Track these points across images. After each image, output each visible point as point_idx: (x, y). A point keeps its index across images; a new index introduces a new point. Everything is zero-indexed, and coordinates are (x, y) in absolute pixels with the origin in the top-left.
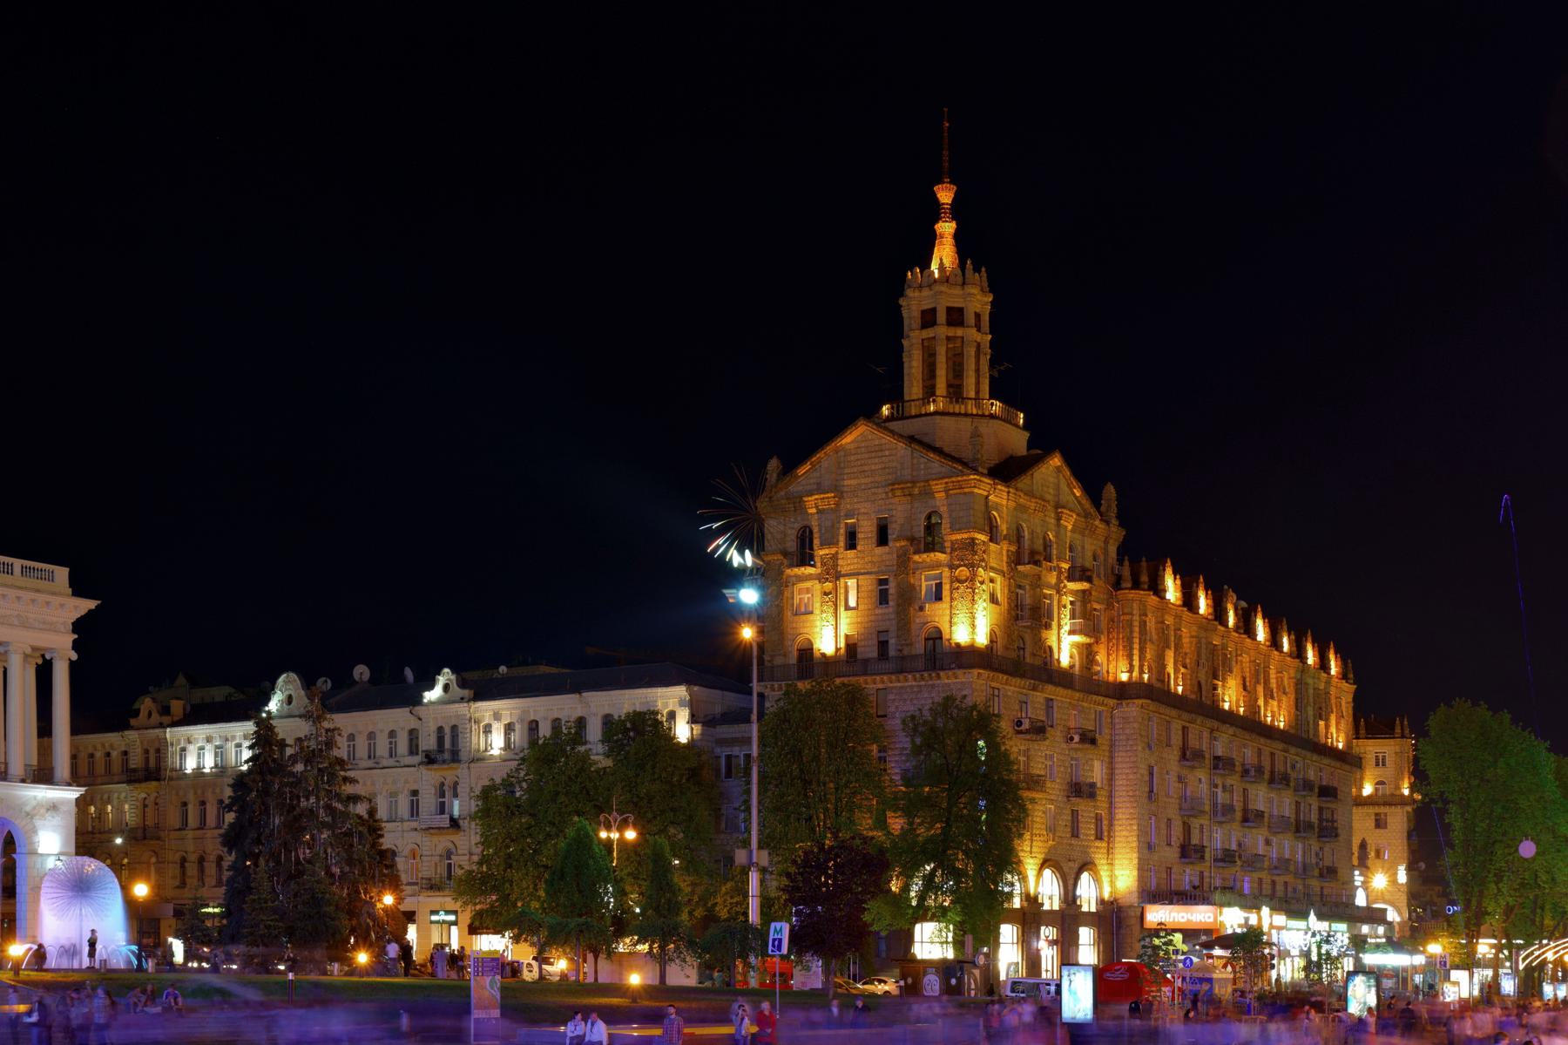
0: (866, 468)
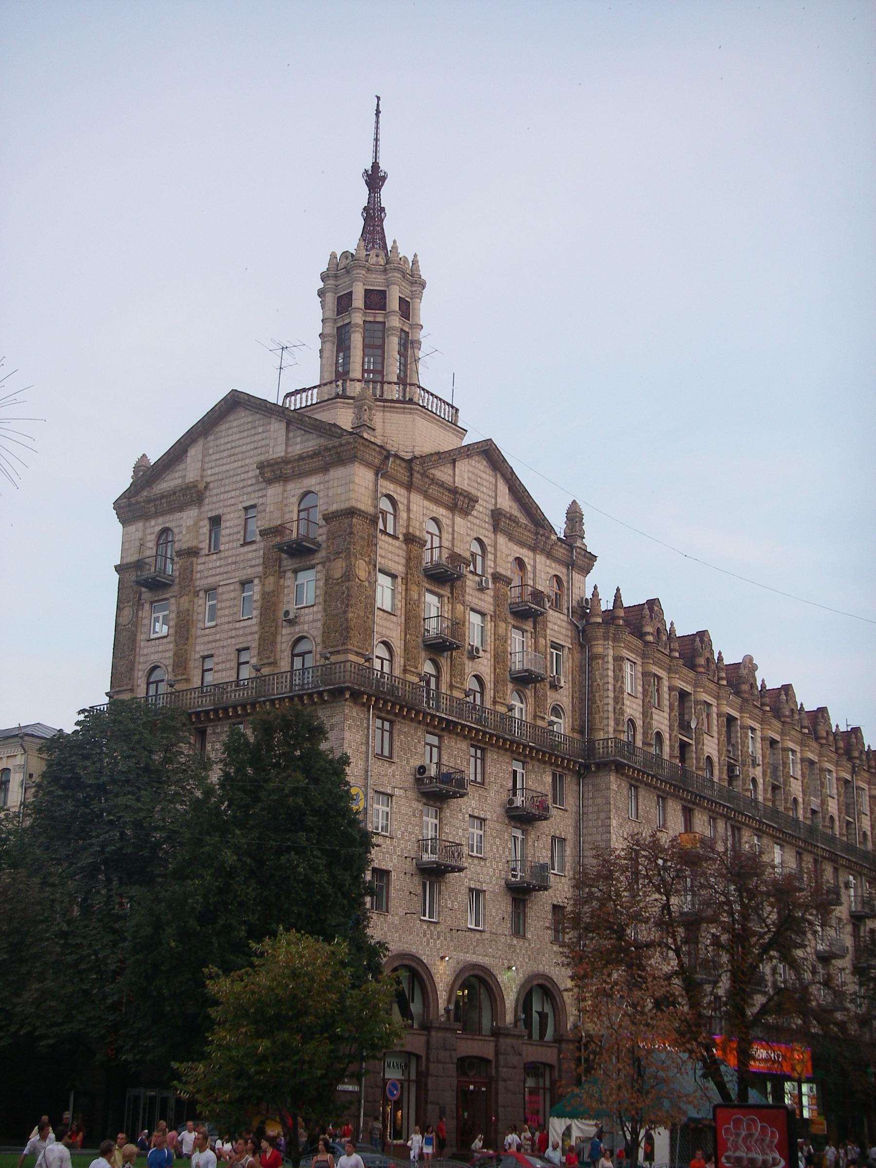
0: (237, 450)
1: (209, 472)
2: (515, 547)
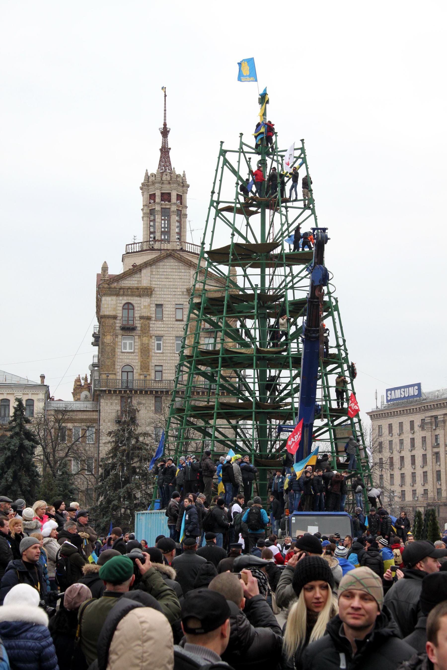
0: (170, 277)
1: (154, 283)
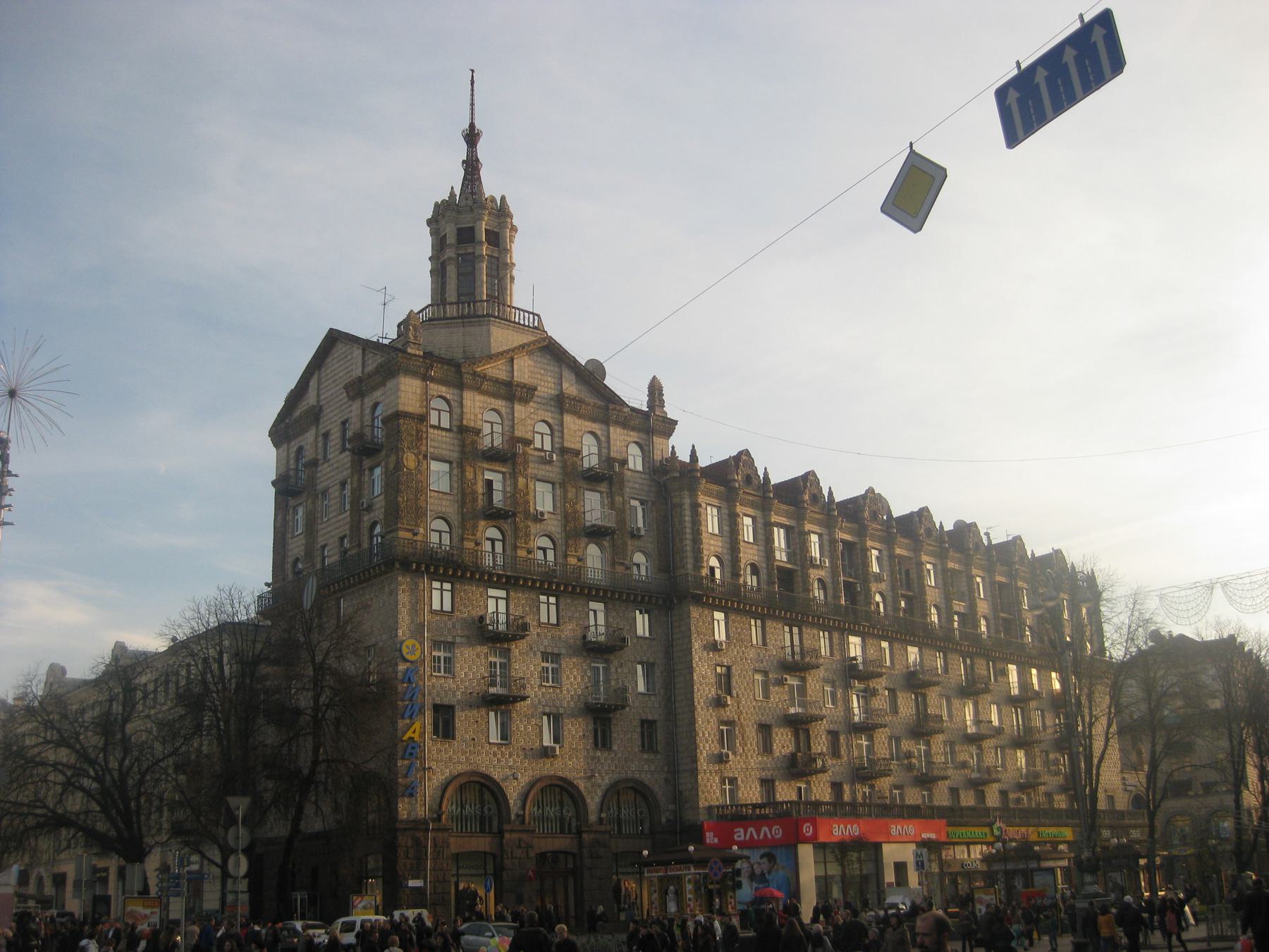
2: (587, 423)
